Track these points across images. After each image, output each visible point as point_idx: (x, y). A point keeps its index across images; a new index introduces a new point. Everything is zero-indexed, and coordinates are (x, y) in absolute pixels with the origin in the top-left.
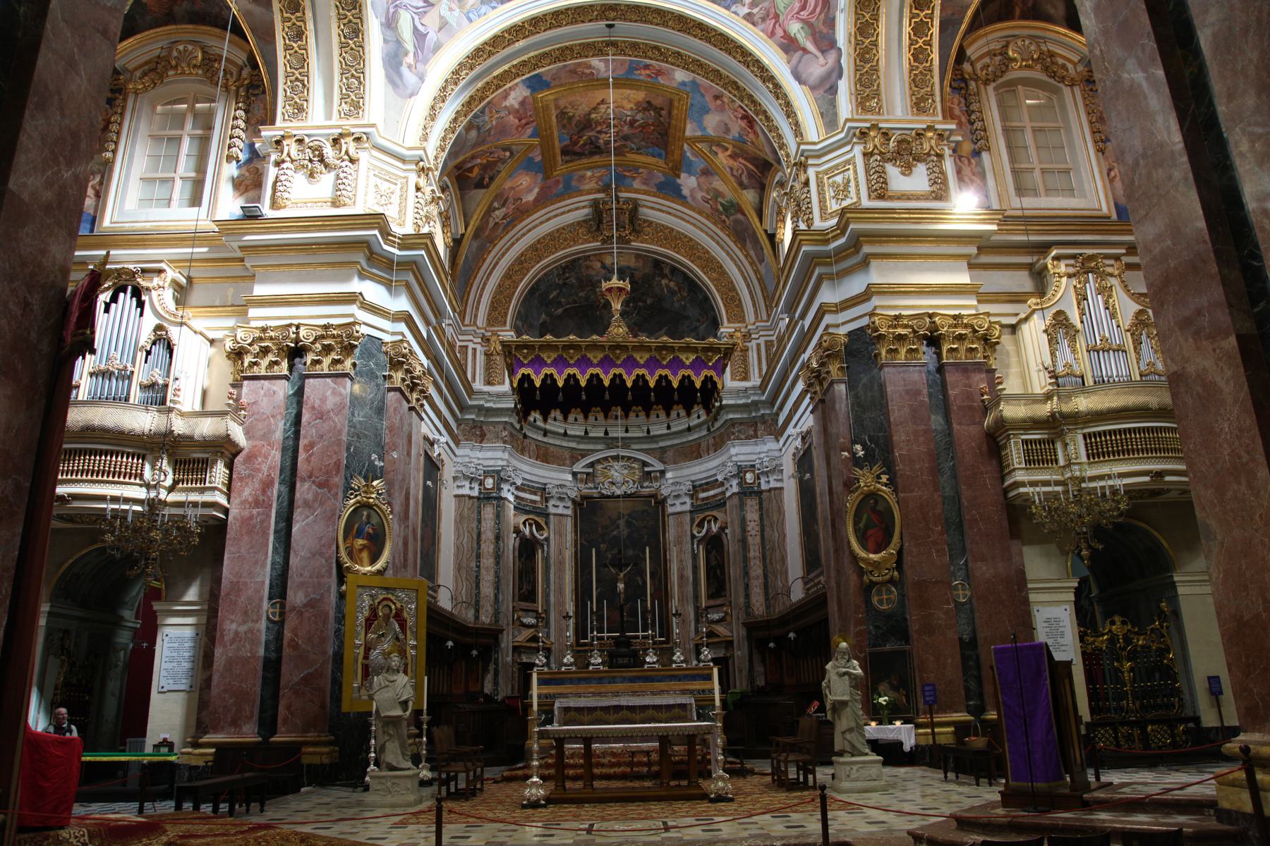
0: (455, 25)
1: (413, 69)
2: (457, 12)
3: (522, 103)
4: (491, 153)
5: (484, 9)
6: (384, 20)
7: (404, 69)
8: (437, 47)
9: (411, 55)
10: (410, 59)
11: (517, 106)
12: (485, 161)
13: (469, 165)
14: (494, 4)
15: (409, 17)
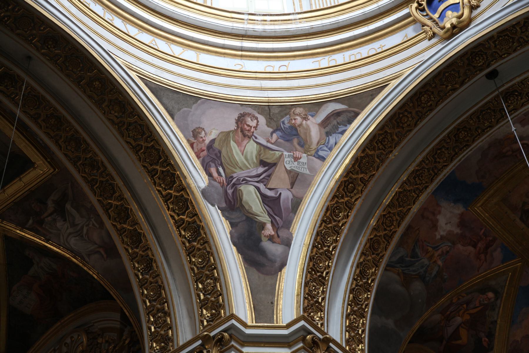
0: (308, 172)
1: (276, 239)
2: (304, 158)
3: (462, 223)
4: (468, 303)
5: (332, 140)
6: (224, 205)
7: (266, 245)
8: (297, 203)
9: (269, 226)
10: (269, 230)
11: (457, 231)
12: (467, 317)
13: (450, 330)
14: (340, 130)
15: (252, 189)
